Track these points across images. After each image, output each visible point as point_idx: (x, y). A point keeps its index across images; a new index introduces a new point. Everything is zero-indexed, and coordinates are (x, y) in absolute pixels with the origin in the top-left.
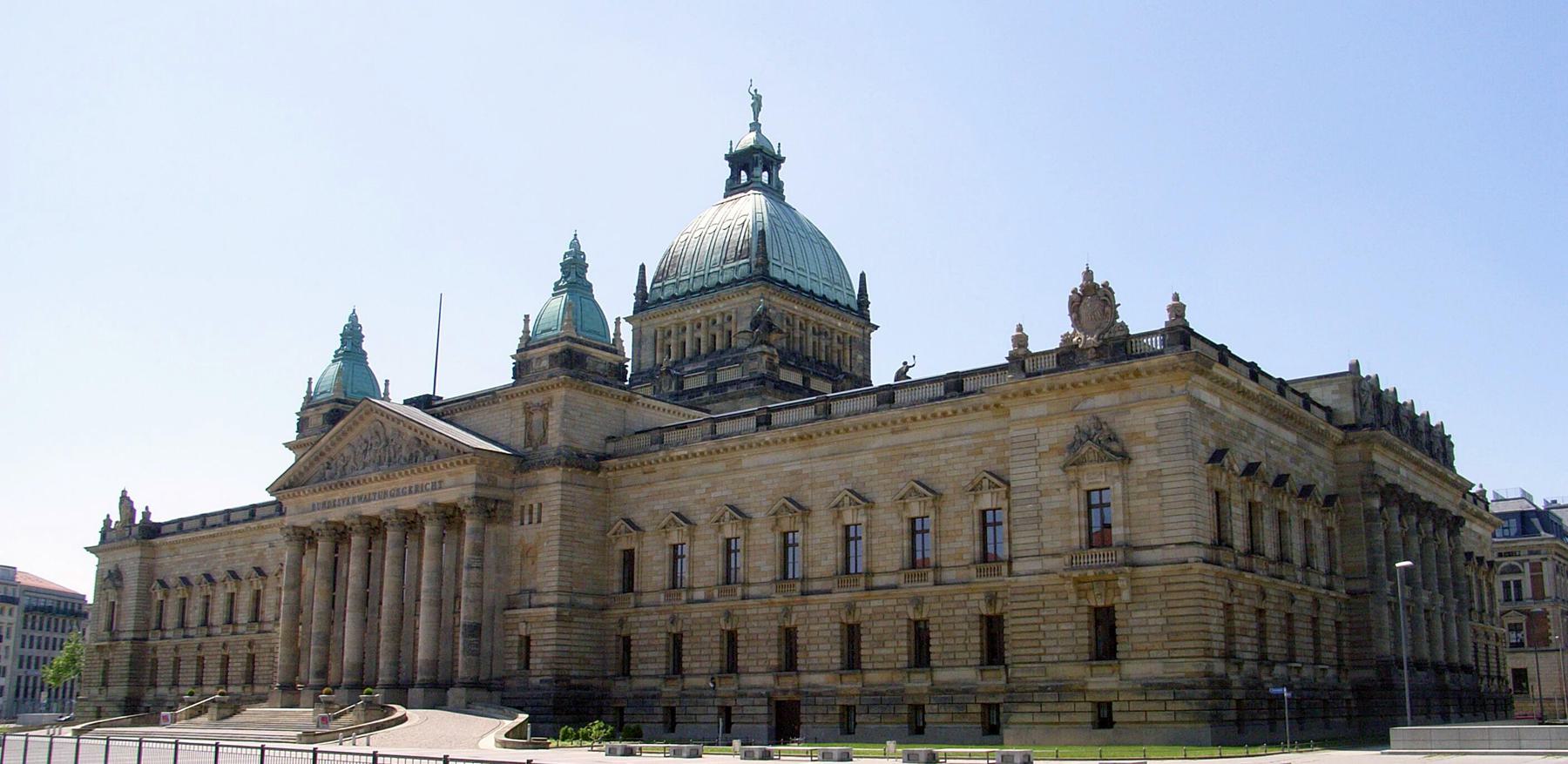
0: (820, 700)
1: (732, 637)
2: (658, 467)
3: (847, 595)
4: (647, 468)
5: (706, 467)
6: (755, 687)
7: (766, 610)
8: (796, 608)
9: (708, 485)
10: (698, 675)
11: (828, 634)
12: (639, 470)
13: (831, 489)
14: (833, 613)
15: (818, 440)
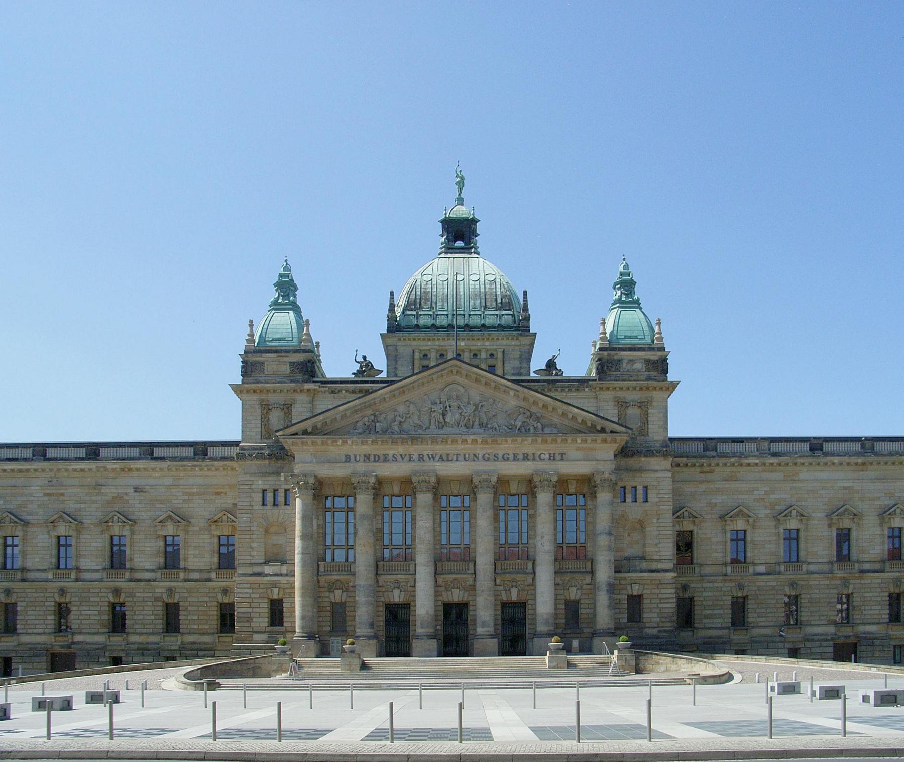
0: (877, 642)
1: (795, 599)
2: (717, 469)
3: (898, 574)
4: (707, 469)
5: (766, 475)
6: (818, 635)
7: (827, 582)
8: (853, 581)
9: (767, 488)
10: (764, 627)
11: (879, 599)
12: (698, 470)
13: (877, 503)
14: (883, 585)
15: (870, 467)
